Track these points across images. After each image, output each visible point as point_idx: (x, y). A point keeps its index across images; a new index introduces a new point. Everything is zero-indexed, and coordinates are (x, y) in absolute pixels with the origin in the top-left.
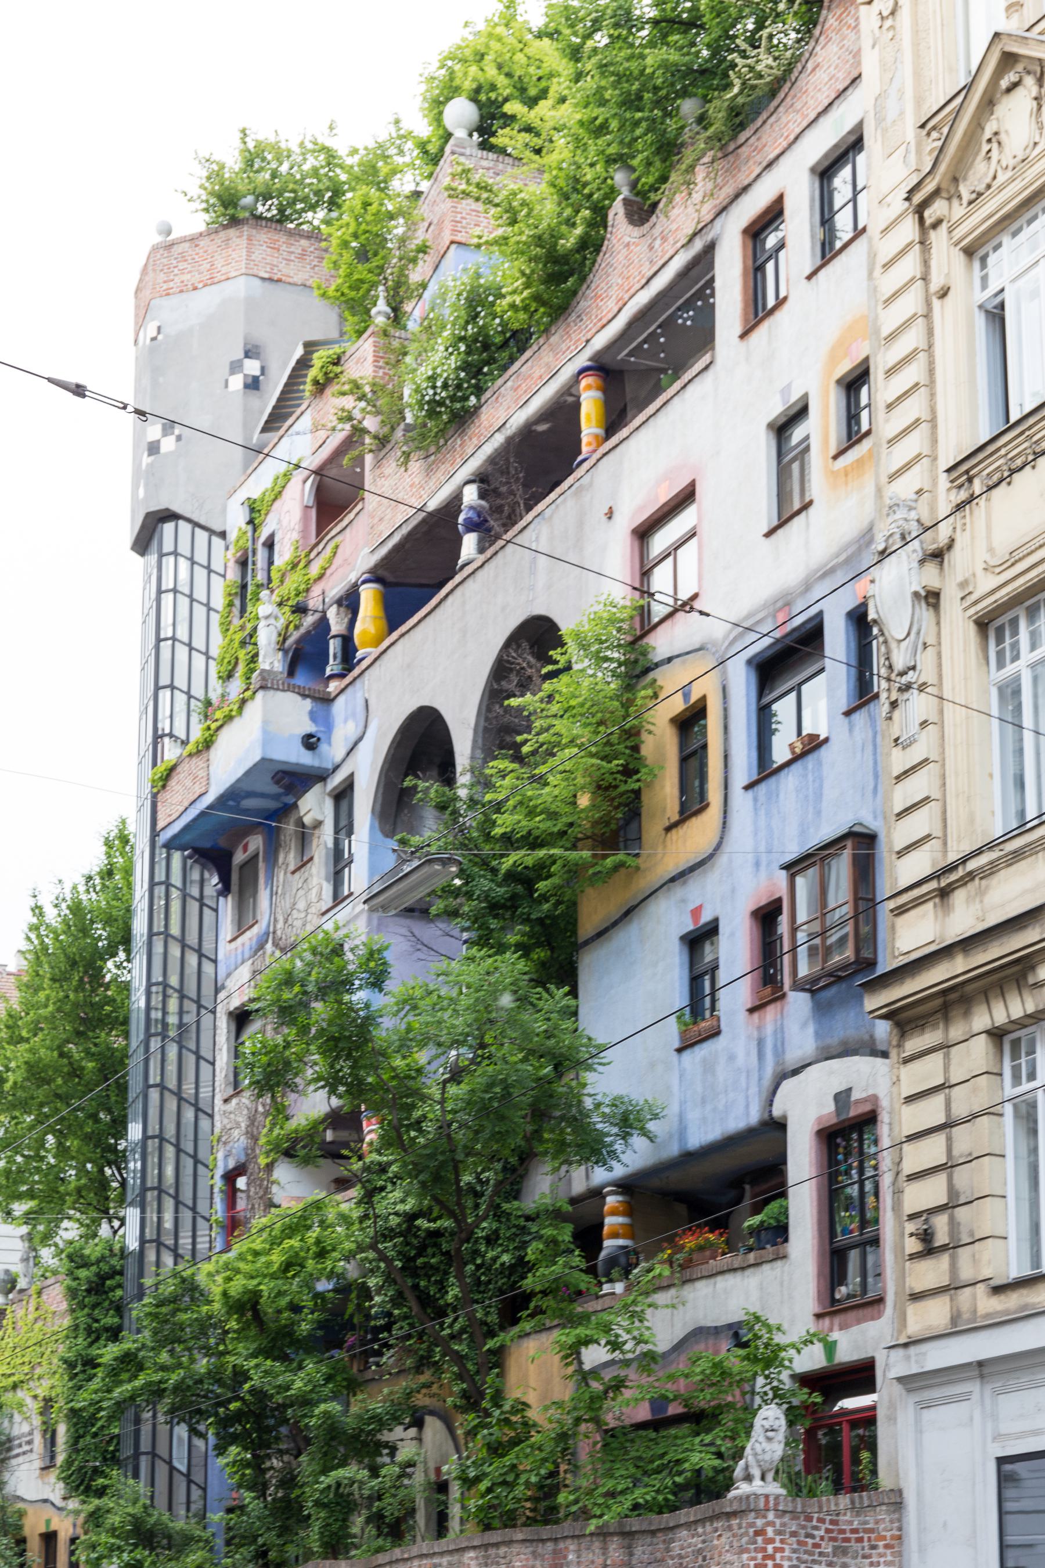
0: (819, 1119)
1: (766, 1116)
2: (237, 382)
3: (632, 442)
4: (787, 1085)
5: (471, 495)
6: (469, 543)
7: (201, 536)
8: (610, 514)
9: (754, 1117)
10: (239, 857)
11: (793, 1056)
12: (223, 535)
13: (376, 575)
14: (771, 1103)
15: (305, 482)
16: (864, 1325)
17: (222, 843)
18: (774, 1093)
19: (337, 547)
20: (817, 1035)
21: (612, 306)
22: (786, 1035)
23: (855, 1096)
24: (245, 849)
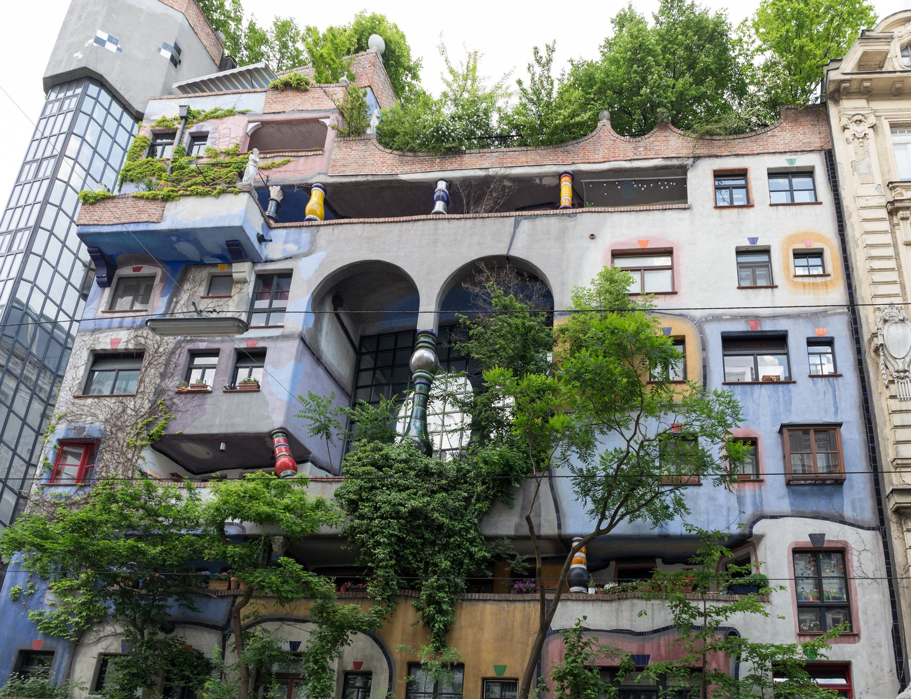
0: (796, 543)
1: (747, 532)
2: (167, 54)
3: (616, 216)
4: (763, 521)
5: (442, 185)
6: (439, 206)
7: (116, 109)
8: (592, 236)
9: (735, 530)
10: (126, 271)
11: (769, 509)
12: (138, 117)
13: (325, 187)
14: (751, 527)
15: (249, 122)
16: (841, 645)
17: (119, 259)
18: (754, 522)
19: (289, 161)
20: (792, 504)
21: (599, 157)
22: (764, 499)
23: (826, 538)
24: (139, 269)
